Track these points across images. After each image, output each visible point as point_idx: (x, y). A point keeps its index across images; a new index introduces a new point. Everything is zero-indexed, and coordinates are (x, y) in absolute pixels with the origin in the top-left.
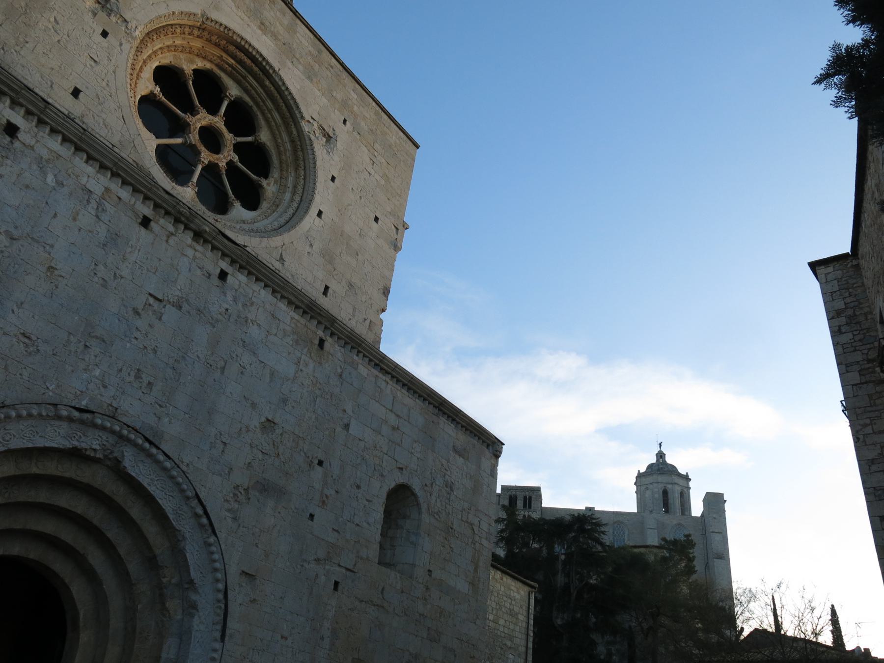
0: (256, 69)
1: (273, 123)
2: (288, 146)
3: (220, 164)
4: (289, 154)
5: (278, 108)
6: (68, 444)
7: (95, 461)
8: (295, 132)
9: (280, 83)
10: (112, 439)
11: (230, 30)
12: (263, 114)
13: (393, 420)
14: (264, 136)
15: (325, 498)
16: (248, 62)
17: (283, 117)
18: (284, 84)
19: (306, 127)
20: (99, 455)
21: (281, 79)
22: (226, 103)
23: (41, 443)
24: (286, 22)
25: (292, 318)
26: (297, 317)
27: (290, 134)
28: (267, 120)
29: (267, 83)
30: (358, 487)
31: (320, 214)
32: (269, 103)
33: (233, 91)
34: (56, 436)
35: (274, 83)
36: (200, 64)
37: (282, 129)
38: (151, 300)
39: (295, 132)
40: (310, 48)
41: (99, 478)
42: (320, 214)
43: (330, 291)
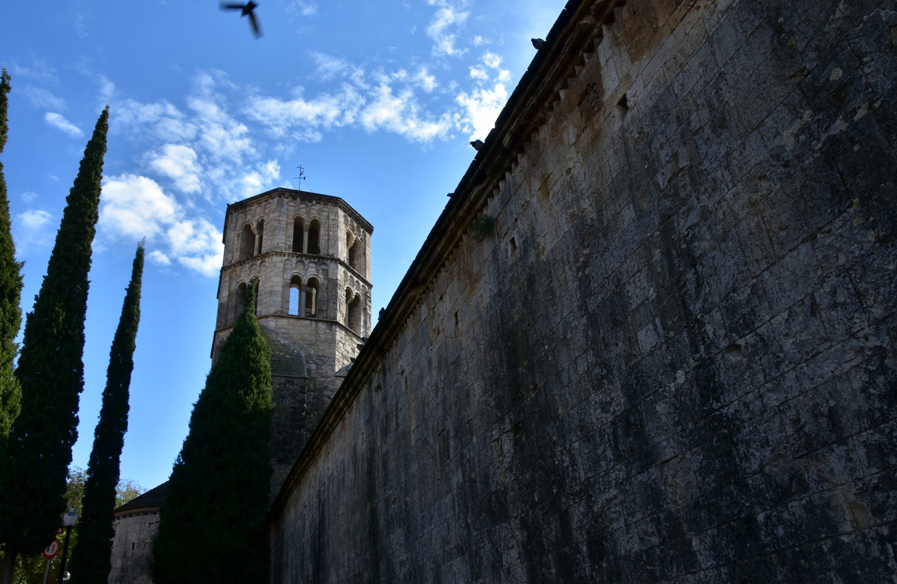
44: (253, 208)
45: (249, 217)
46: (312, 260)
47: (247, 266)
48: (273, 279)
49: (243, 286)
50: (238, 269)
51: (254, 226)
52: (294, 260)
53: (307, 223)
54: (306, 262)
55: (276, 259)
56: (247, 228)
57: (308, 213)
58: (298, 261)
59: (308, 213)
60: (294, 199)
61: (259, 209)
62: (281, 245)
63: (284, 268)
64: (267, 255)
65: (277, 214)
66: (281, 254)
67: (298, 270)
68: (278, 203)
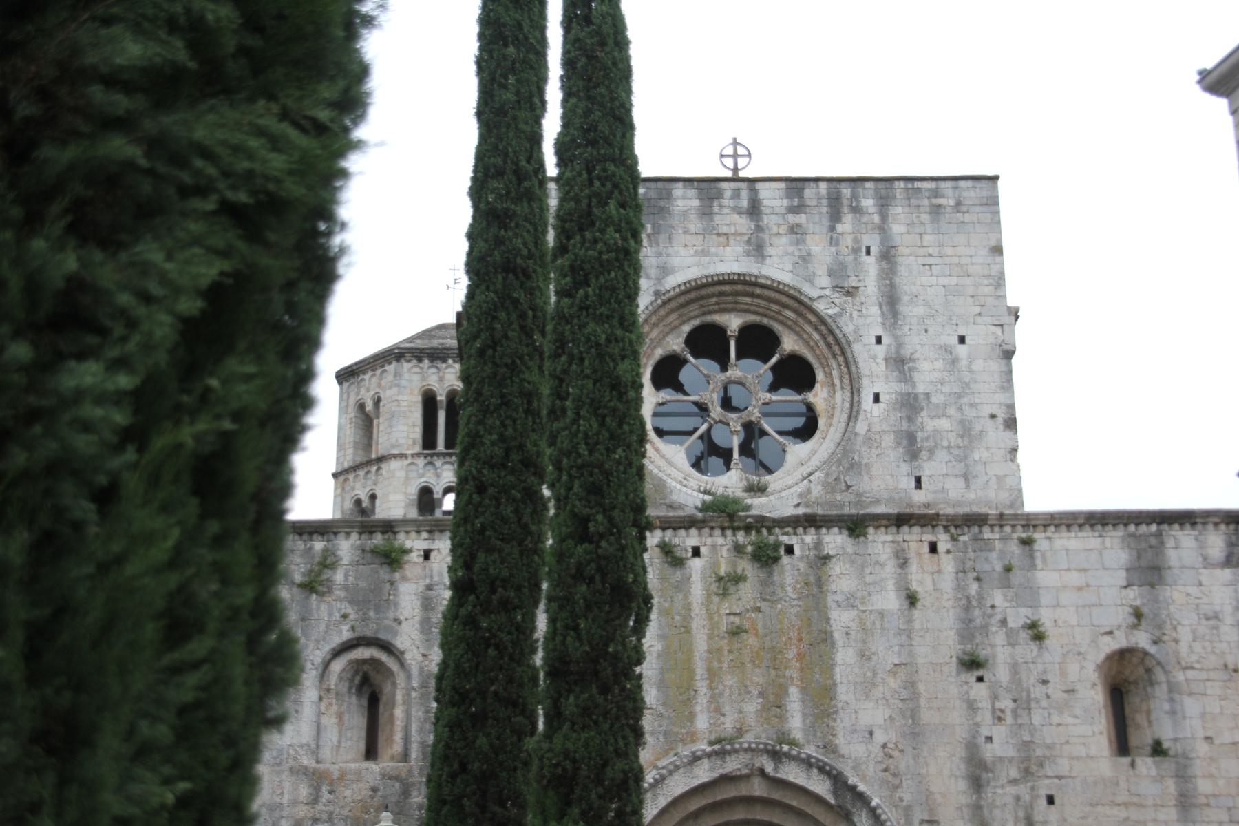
0: (739, 287)
1: (790, 323)
2: (816, 336)
3: (753, 419)
4: (821, 344)
5: (786, 306)
6: (716, 775)
7: (747, 777)
8: (813, 319)
9: (769, 283)
10: (748, 756)
11: (689, 282)
12: (776, 320)
13: (1075, 578)
14: (789, 343)
15: (999, 713)
16: (727, 288)
17: (795, 311)
18: (773, 281)
19: (820, 306)
20: (745, 771)
21: (767, 278)
22: (733, 344)
23: (696, 782)
24: (745, 203)
25: (884, 542)
26: (889, 538)
27: (810, 322)
28: (782, 323)
29: (758, 291)
30: (1045, 682)
31: (877, 399)
32: (775, 307)
33: (733, 323)
34: (704, 773)
35: (763, 286)
36: (687, 328)
37: (801, 321)
38: (732, 618)
39: (813, 319)
40: (785, 202)
41: (758, 788)
42: (877, 399)
43: (923, 479)
44: (367, 377)
45: (363, 391)
46: (448, 459)
47: (361, 473)
48: (391, 497)
49: (358, 502)
50: (351, 477)
51: (369, 407)
52: (421, 462)
53: (441, 398)
54: (438, 463)
55: (394, 465)
56: (361, 407)
57: (441, 380)
58: (427, 464)
59: (441, 380)
60: (420, 360)
61: (374, 380)
62: (402, 441)
63: (407, 478)
64: (381, 459)
65: (395, 390)
66: (402, 456)
67: (429, 478)
68: (397, 374)
